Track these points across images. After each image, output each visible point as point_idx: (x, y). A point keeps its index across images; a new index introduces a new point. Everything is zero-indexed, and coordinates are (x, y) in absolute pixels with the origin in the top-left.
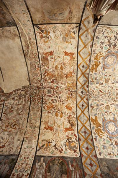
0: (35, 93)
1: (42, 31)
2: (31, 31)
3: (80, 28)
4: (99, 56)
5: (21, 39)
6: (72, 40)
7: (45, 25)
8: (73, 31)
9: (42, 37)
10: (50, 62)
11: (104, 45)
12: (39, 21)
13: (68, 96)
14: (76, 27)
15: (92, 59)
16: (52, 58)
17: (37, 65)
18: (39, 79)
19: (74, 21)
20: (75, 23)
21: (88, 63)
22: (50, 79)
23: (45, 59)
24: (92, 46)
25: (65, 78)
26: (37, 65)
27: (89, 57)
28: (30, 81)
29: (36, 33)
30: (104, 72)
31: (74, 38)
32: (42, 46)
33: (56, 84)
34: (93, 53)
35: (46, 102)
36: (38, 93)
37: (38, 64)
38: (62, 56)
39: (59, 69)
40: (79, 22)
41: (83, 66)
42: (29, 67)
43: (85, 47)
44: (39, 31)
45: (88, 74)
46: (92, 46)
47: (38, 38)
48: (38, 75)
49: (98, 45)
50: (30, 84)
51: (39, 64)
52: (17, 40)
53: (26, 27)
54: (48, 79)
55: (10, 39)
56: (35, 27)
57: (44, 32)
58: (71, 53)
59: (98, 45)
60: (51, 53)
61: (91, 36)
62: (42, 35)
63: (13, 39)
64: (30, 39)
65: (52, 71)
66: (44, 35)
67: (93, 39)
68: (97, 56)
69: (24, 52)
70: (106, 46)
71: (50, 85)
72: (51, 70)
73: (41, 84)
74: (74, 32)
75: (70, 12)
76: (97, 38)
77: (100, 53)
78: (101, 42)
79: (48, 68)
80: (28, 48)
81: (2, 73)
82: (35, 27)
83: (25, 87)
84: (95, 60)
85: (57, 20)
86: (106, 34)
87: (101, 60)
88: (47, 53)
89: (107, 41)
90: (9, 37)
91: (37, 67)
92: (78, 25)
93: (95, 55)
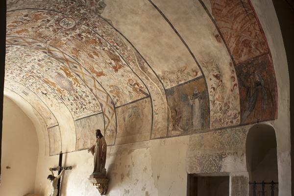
0: (80, 10)
1: (140, 90)
2: (151, 87)
3: (112, 103)
4: (77, 83)
5: (156, 75)
6: (110, 90)
7: (140, 98)
8: (116, 98)
9: (137, 84)
10: (109, 58)
11: (84, 95)
12: (146, 102)
13: (43, 35)
14: (116, 103)
15: (78, 78)
16: (111, 63)
17: (118, 47)
18: (97, 29)
19: (120, 109)
20: (118, 107)
21: (77, 73)
22: (87, 37)
23: (116, 59)
24: (91, 90)
25: (74, 47)
26: (118, 47)
27: (82, 78)
28: (105, 20)
29: (145, 87)
30: (54, 71)
31: (111, 92)
32: (130, 75)
33: (73, 35)
34: (84, 84)
35: (51, 15)
36: (76, 12)
37: (117, 48)
38: (104, 70)
39: (92, 54)
40: (116, 109)
41: (76, 67)
42: (125, 41)
43: (95, 86)
44: (143, 89)
45: (63, 63)
46: (91, 90)
47: (139, 81)
48: (104, 34)
49: (88, 93)
50: (99, 16)
51: (117, 50)
52: (159, 73)
53: (155, 89)
54: (89, 36)
55: (168, 72)
56: (148, 93)
57: (138, 90)
58: (99, 76)
59: (88, 93)
60: (116, 70)
61: (100, 99)
62: (138, 85)
63: (164, 72)
64: (147, 79)
65: (96, 47)
66: (136, 86)
67: (96, 96)
68: (78, 83)
69: (144, 61)
70: (82, 95)
71: (78, 31)
72: (98, 48)
73: (88, 25)
74: (115, 97)
75: (124, 119)
76: (95, 99)
77: (79, 86)
78: (88, 96)
79: (104, 49)
80: (142, 68)
81: (155, 6)
82: (148, 93)
83: (101, 7)
84: (74, 77)
85: (133, 107)
86: (91, 104)
87: (71, 79)
88: (120, 68)
89: (86, 99)
90: (170, 73)
91: (115, 45)
92: (116, 106)
93: (81, 83)
